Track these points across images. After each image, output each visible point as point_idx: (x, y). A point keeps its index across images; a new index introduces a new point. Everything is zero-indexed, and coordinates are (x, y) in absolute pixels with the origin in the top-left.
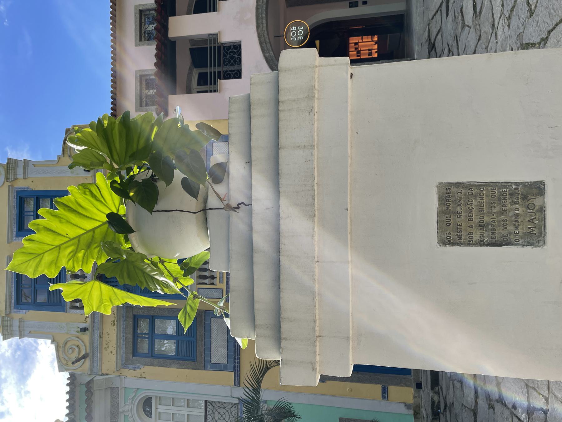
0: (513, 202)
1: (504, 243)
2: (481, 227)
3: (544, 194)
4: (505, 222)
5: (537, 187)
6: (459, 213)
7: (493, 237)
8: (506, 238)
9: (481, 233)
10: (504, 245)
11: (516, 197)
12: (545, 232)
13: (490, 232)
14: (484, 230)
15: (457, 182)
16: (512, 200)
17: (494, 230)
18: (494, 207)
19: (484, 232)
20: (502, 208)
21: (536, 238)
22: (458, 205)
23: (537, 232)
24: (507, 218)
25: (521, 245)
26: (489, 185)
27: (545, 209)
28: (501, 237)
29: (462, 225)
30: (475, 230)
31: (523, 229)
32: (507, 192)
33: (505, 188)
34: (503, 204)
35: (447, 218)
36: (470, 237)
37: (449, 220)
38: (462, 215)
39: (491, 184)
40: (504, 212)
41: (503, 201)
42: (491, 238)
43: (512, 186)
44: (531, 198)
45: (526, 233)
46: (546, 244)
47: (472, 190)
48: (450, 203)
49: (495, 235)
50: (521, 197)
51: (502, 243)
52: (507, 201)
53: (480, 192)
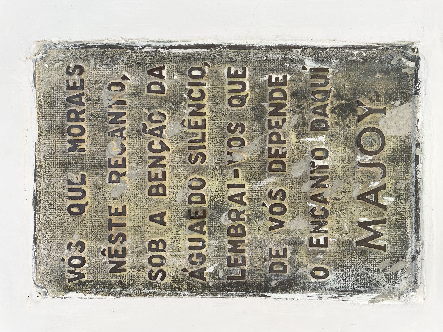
0: (305, 124)
1: (273, 284)
2: (195, 221)
3: (417, 93)
4: (277, 201)
5: (392, 69)
6: (117, 165)
7: (236, 260)
8: (282, 264)
9: (194, 244)
10: (274, 290)
11: (318, 104)
12: (418, 239)
13: (226, 239)
14: (204, 233)
15: (104, 43)
16: (304, 118)
17: (239, 232)
18: (239, 143)
19: (203, 241)
20: (268, 145)
21: (387, 263)
22: (112, 134)
23: (389, 240)
24: (285, 184)
25: (332, 289)
26: (221, 55)
27: (418, 152)
28: (265, 260)
29: (124, 213)
30: (174, 230)
31: (341, 229)
32: (284, 84)
33: (277, 71)
34: (271, 131)
35: (74, 184)
36: (155, 261)
37: (80, 194)
38: (124, 174)
39: (230, 53)
40: (274, 162)
41: (270, 121)
42: (229, 265)
43: (302, 61)
44: (371, 111)
45: (350, 242)
46: (421, 288)
47: (161, 76)
48: (83, 124)
49: (244, 251)
50: (335, 105)
51: (267, 282)
52: (284, 121)
53: (190, 84)
